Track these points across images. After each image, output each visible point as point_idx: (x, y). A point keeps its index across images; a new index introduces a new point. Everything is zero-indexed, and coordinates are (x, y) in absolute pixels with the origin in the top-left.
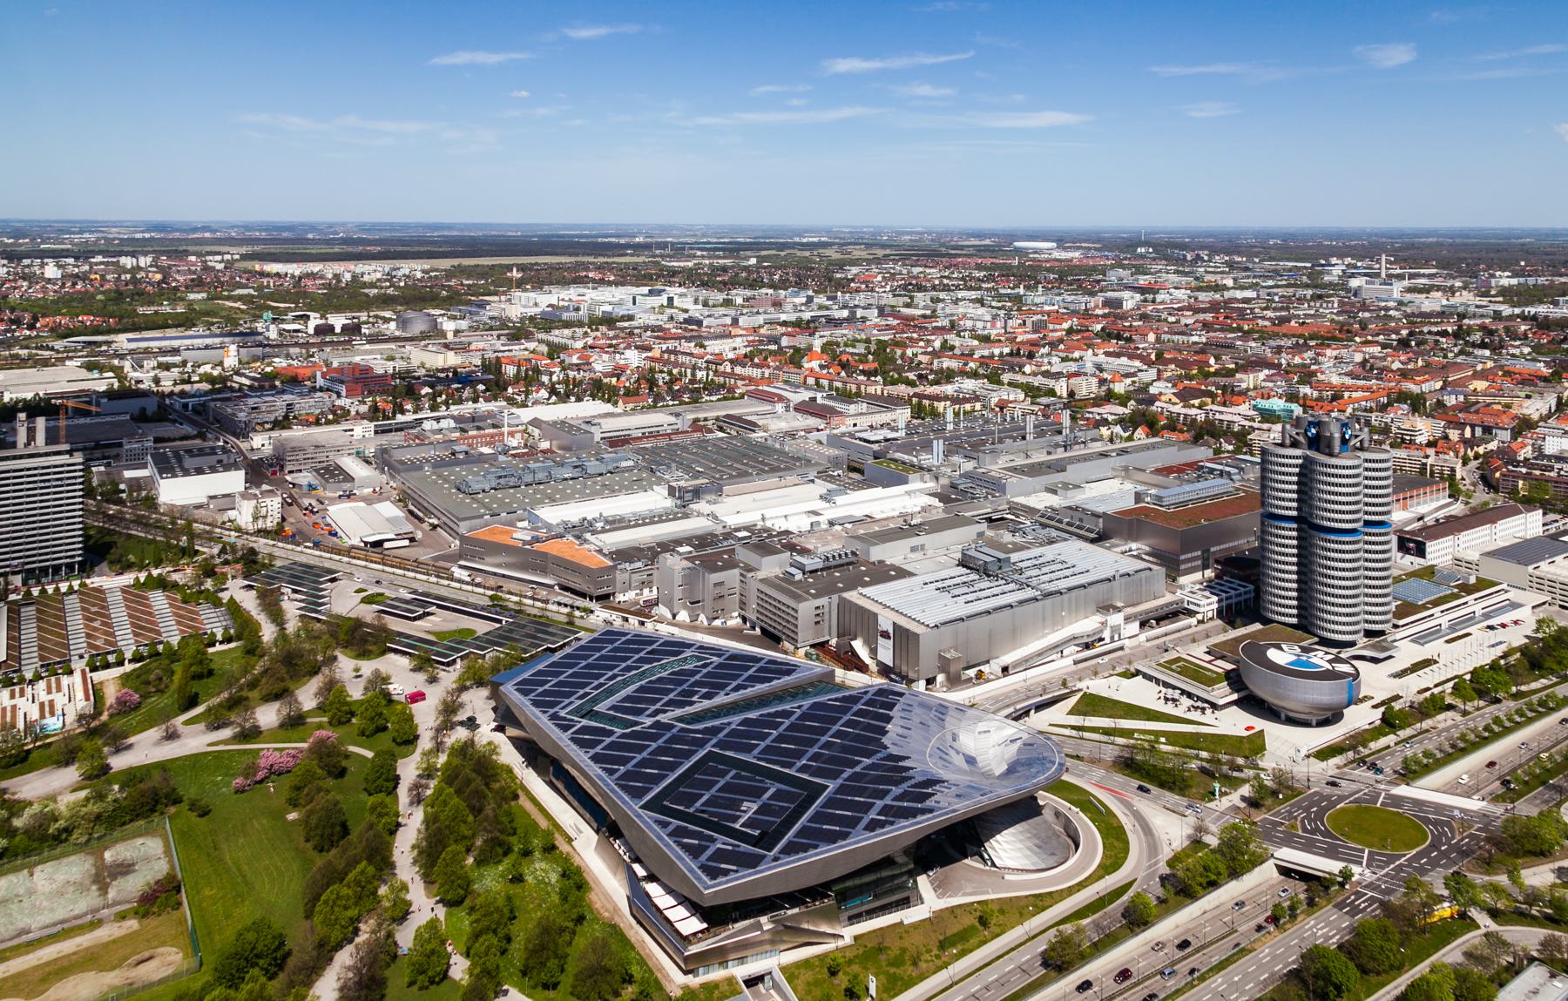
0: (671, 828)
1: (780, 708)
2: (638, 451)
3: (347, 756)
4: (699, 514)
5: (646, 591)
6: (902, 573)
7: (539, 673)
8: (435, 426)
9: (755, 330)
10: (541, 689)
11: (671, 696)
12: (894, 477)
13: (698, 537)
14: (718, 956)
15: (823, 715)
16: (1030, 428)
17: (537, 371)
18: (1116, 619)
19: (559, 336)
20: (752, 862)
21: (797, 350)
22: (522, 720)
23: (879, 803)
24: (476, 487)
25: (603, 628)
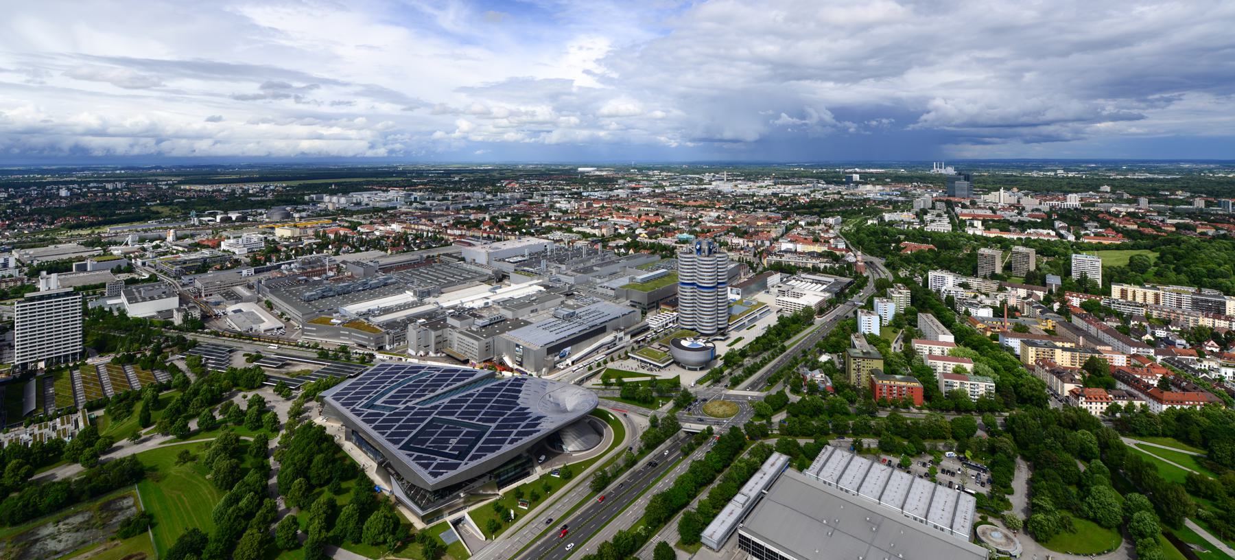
6: (527, 323)
15: (489, 393)
19: (355, 219)
20: (455, 466)
23: (515, 431)
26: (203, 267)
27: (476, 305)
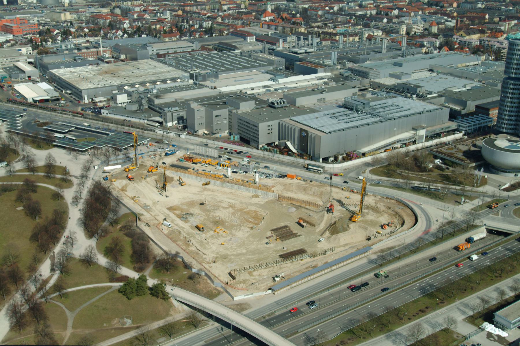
3: (37, 186)
12: (309, 70)
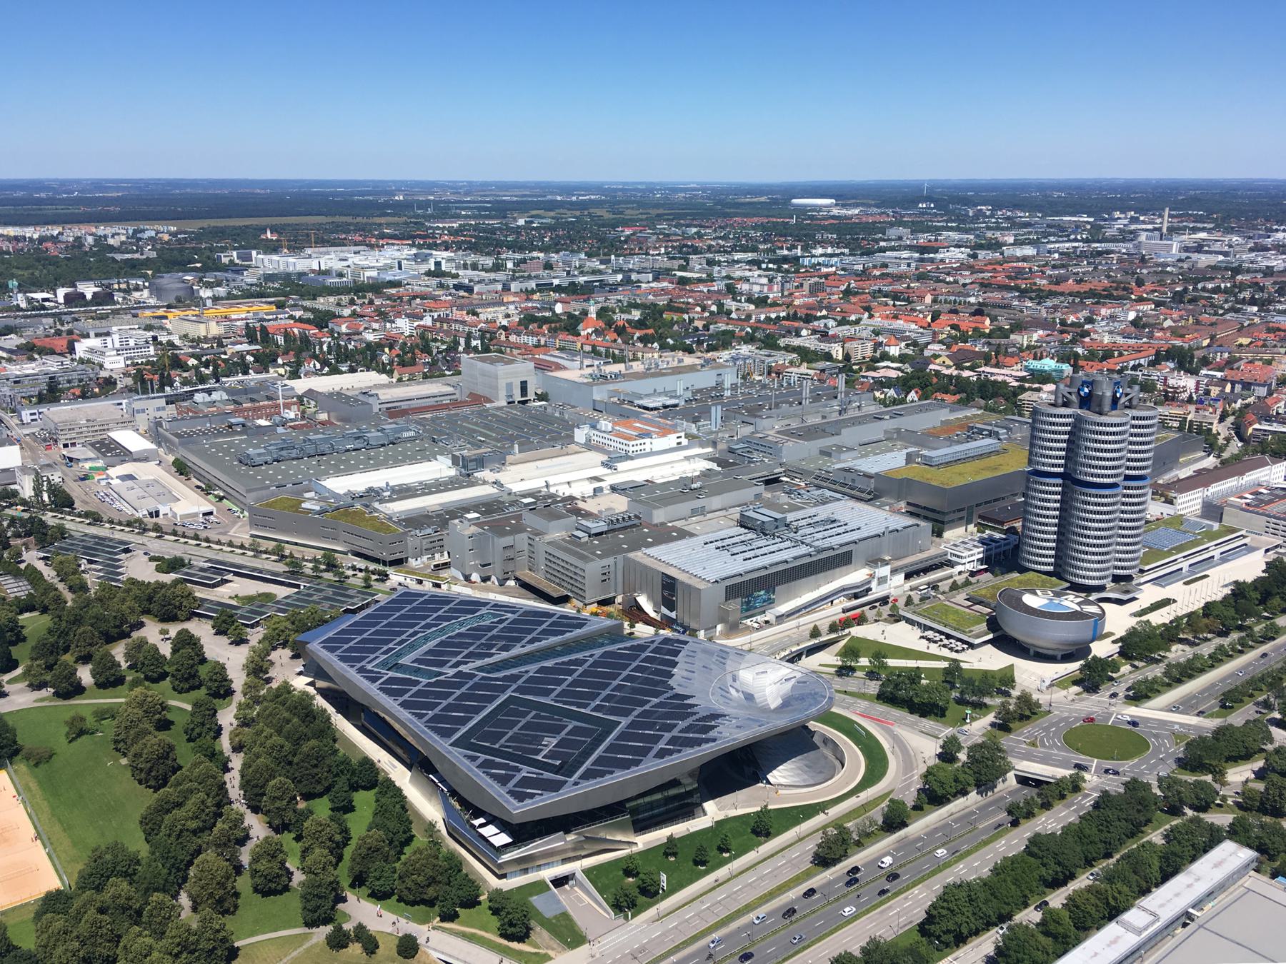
0: (479, 761)
1: (573, 657)
2: (417, 423)
4: (485, 482)
5: (437, 556)
7: (343, 632)
8: (208, 399)
9: (528, 293)
10: (346, 646)
11: (471, 649)
13: (484, 504)
14: (524, 864)
16: (806, 392)
17: (305, 339)
18: (884, 571)
19: (323, 303)
21: (570, 316)
22: (331, 674)
24: (258, 460)
25: (401, 590)
26: (51, 393)
27: (576, 491)
